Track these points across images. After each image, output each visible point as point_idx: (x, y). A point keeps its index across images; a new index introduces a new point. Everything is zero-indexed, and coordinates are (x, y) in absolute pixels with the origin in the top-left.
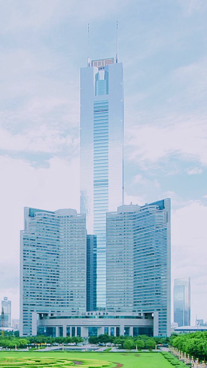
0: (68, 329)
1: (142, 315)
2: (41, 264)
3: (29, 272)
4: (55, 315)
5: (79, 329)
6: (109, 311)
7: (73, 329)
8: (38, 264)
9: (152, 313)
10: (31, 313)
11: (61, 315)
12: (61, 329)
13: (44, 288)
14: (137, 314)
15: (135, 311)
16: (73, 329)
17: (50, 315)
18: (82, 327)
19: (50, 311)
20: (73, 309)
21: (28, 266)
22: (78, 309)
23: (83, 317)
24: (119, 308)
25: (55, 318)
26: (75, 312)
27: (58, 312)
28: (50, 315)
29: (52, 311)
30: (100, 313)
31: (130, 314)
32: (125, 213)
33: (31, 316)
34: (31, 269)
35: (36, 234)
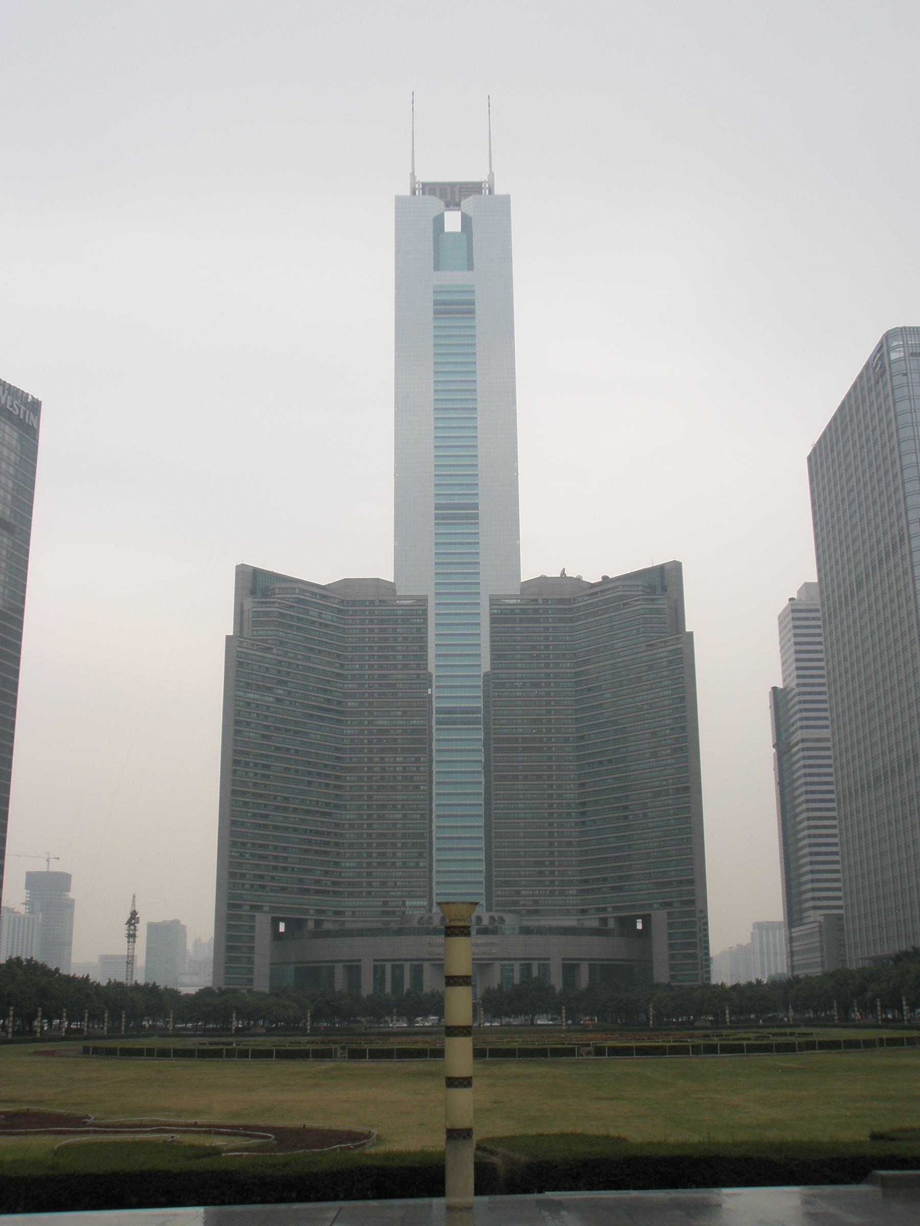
0: (378, 971)
1: (611, 924)
2: (288, 750)
3: (251, 775)
4: (327, 926)
5: (417, 972)
6: (505, 911)
7: (398, 969)
8: (278, 749)
9: (633, 920)
10: (253, 918)
11: (348, 926)
12: (353, 970)
13: (296, 830)
14: (592, 922)
15: (584, 911)
16: (398, 969)
17: (311, 925)
18: (426, 966)
19: (312, 912)
20: (385, 904)
21: (248, 753)
22: (404, 902)
23: (420, 932)
24: (536, 902)
25: (327, 934)
26: (394, 913)
27: (336, 913)
28: (311, 925)
29: (317, 911)
30: (479, 919)
31: (571, 922)
32: (546, 601)
33: (252, 928)
34: (256, 765)
35: (275, 651)
